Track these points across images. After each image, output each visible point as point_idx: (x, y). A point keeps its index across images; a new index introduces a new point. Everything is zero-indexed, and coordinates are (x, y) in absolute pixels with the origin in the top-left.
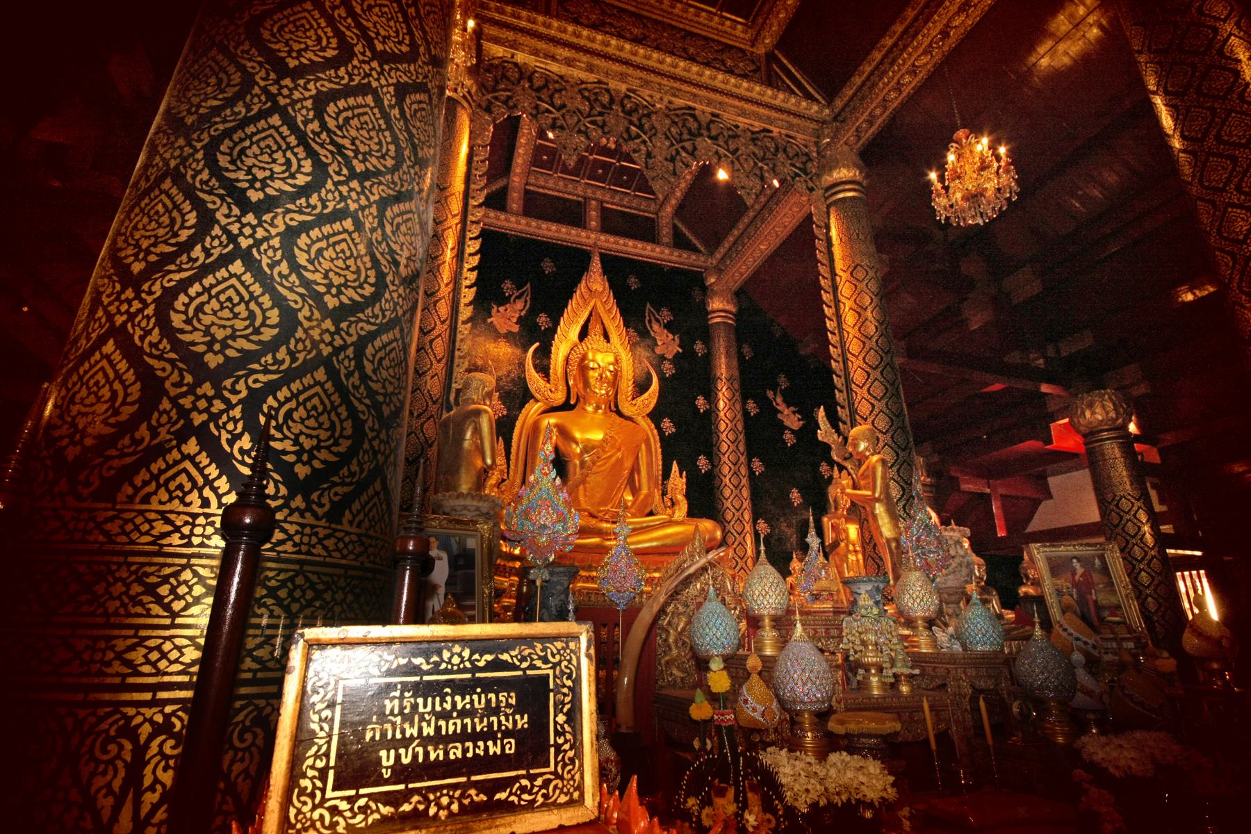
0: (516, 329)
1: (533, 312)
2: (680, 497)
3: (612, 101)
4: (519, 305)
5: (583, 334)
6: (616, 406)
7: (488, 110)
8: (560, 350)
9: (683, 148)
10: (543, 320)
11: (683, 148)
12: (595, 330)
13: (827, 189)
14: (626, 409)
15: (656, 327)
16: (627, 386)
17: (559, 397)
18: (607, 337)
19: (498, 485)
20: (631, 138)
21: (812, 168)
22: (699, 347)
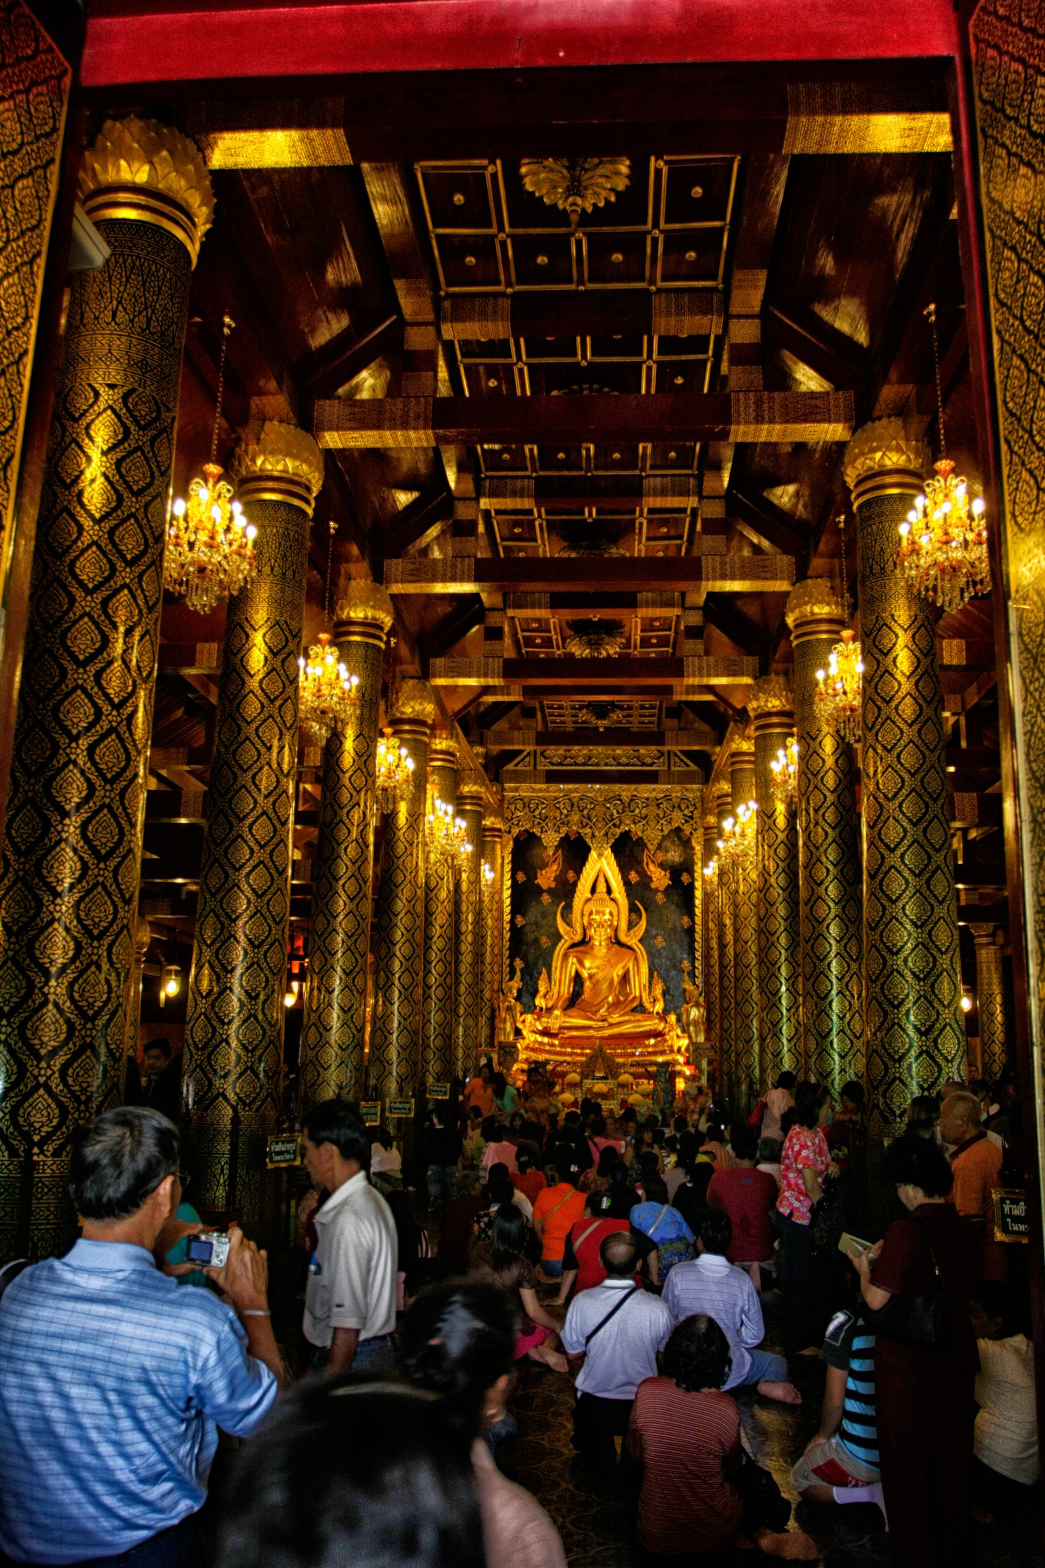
0: (553, 885)
1: (563, 872)
2: (659, 996)
3: (572, 805)
4: (555, 867)
5: (593, 890)
6: (616, 937)
7: (509, 832)
8: (578, 902)
9: (614, 825)
10: (571, 874)
11: (614, 825)
12: (602, 887)
13: (706, 829)
14: (623, 938)
15: (652, 867)
16: (624, 925)
17: (578, 938)
18: (609, 891)
19: (545, 996)
20: (583, 827)
21: (697, 814)
22: (685, 878)
